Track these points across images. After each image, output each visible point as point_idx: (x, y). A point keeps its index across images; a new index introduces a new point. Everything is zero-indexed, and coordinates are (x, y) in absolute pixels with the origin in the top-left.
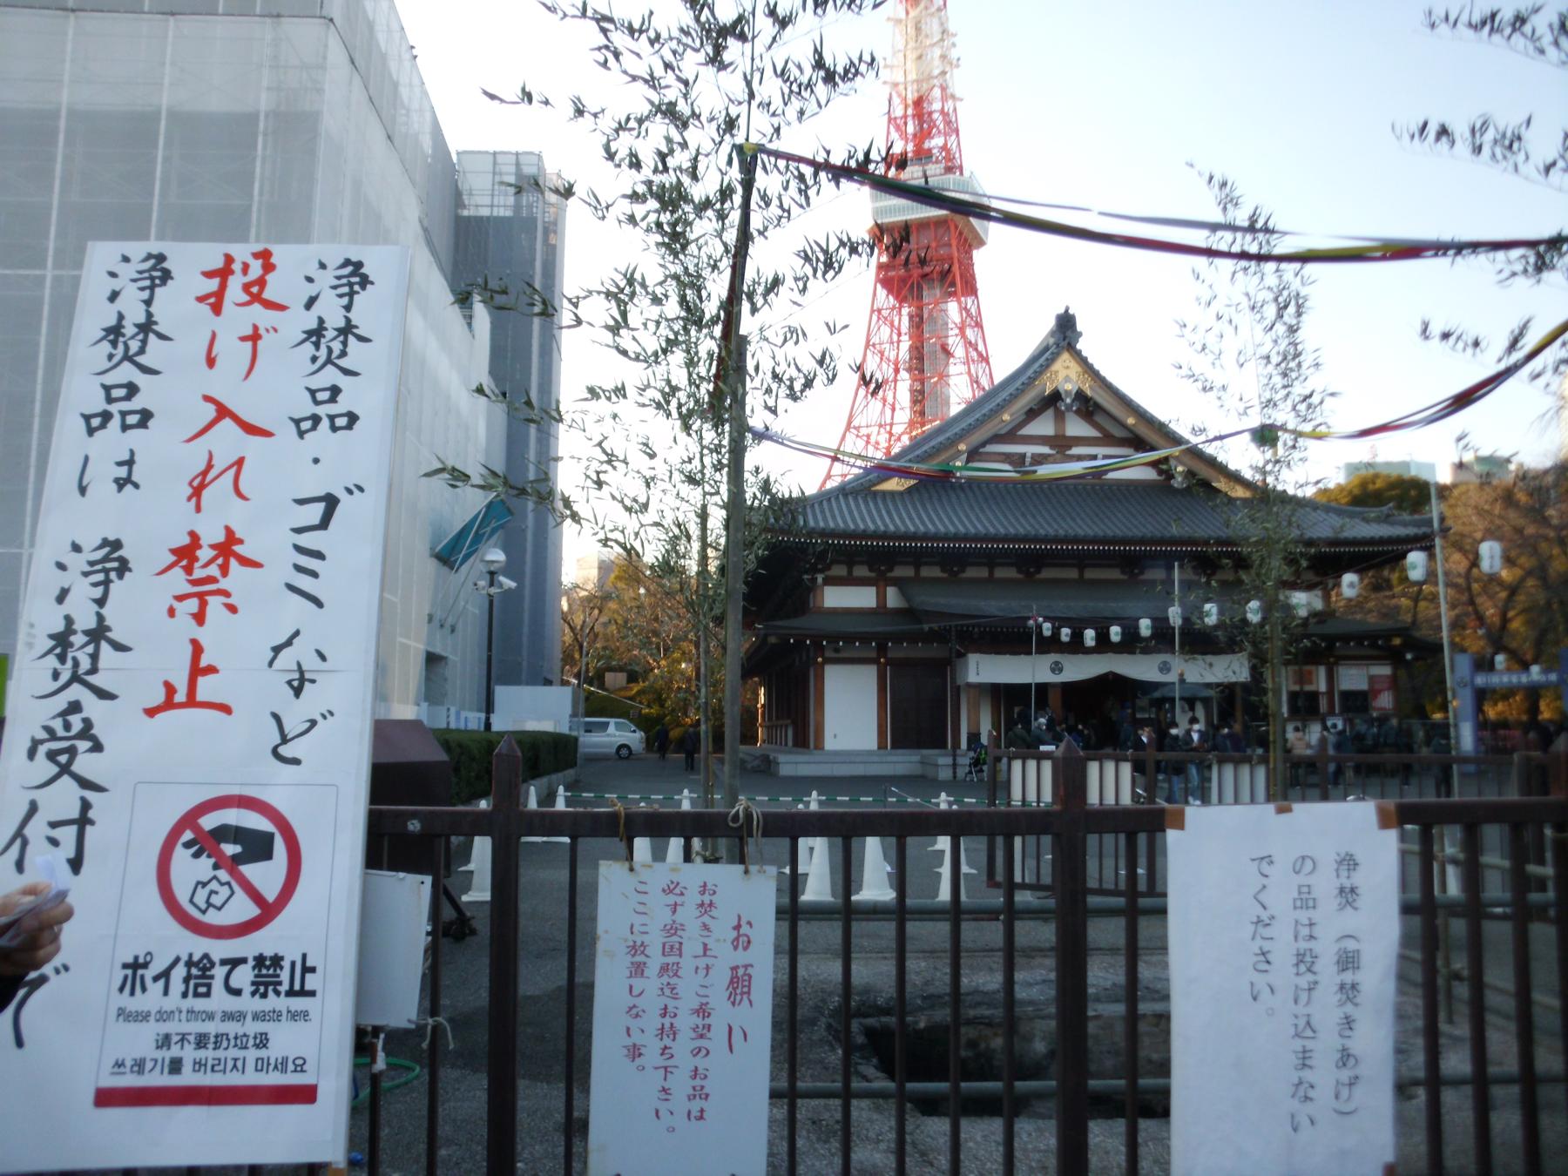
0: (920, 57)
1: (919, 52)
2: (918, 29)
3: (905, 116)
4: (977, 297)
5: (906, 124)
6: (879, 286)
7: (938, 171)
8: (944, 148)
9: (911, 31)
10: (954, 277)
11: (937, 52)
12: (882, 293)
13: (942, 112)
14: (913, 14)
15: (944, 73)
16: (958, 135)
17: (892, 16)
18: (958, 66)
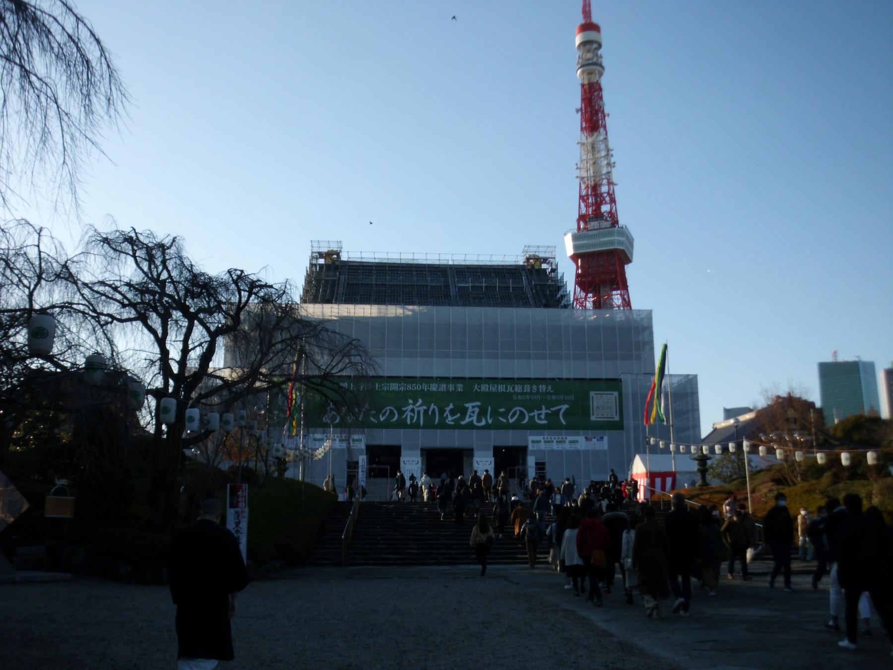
0: (594, 163)
1: (594, 161)
2: (593, 148)
3: (587, 195)
4: (627, 290)
5: (588, 199)
6: (577, 286)
7: (608, 226)
8: (610, 212)
9: (590, 148)
10: (618, 282)
11: (605, 162)
12: (578, 289)
13: (608, 193)
14: (590, 140)
15: (609, 173)
16: (615, 204)
17: (580, 141)
18: (614, 167)
